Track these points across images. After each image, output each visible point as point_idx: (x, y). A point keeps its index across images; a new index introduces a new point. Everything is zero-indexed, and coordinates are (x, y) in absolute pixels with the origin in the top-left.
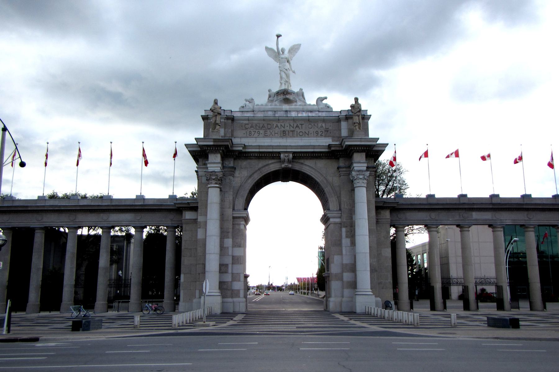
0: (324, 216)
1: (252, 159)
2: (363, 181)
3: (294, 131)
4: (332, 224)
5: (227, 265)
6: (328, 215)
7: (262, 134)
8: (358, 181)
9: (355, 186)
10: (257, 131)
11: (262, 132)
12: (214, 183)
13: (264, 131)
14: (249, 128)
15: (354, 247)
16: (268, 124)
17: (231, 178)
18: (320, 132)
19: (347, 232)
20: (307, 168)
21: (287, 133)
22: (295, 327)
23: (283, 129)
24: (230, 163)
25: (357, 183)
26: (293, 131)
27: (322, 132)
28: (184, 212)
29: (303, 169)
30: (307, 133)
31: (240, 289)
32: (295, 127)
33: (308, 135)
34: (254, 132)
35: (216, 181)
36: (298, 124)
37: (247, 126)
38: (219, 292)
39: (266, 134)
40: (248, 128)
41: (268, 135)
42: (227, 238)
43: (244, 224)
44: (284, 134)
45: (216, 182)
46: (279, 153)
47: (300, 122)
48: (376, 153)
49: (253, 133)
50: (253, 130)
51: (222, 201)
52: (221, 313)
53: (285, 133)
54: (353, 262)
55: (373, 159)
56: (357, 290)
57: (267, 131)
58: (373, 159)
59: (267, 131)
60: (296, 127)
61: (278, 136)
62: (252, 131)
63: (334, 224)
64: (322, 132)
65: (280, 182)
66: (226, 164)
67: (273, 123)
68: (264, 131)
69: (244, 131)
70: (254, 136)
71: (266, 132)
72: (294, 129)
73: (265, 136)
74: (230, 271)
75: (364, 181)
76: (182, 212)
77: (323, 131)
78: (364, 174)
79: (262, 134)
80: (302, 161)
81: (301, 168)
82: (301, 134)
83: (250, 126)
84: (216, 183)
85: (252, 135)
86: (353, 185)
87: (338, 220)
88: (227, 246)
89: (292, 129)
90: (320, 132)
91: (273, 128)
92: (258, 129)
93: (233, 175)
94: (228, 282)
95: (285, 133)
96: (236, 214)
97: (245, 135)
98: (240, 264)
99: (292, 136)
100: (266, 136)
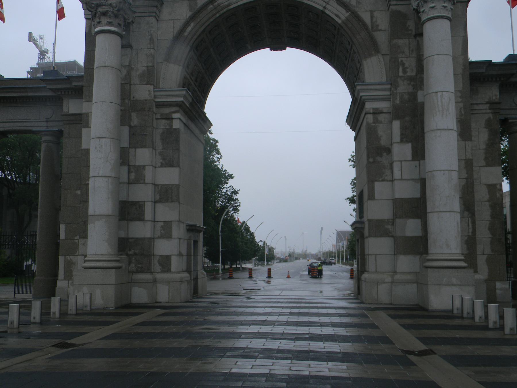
0: (353, 105)
2: (443, 5)
4: (370, 113)
5: (139, 206)
6: (362, 94)
8: (432, 5)
9: (424, 17)
12: (106, 22)
15: (422, 162)
17: (152, 20)
19: (403, 128)
25: (427, 12)
28: (65, 102)
31: (171, 255)
35: (110, 18)
42: (142, 148)
43: (180, 119)
45: (109, 20)
52: (116, 308)
54: (418, 195)
56: (430, 257)
63: (374, 113)
65: (267, 51)
74: (148, 215)
75: (445, 5)
76: (63, 100)
84: (110, 24)
86: (420, 18)
87: (383, 105)
88: (142, 164)
93: (154, 14)
94: (144, 239)
96: (161, 96)
98: (172, 202)
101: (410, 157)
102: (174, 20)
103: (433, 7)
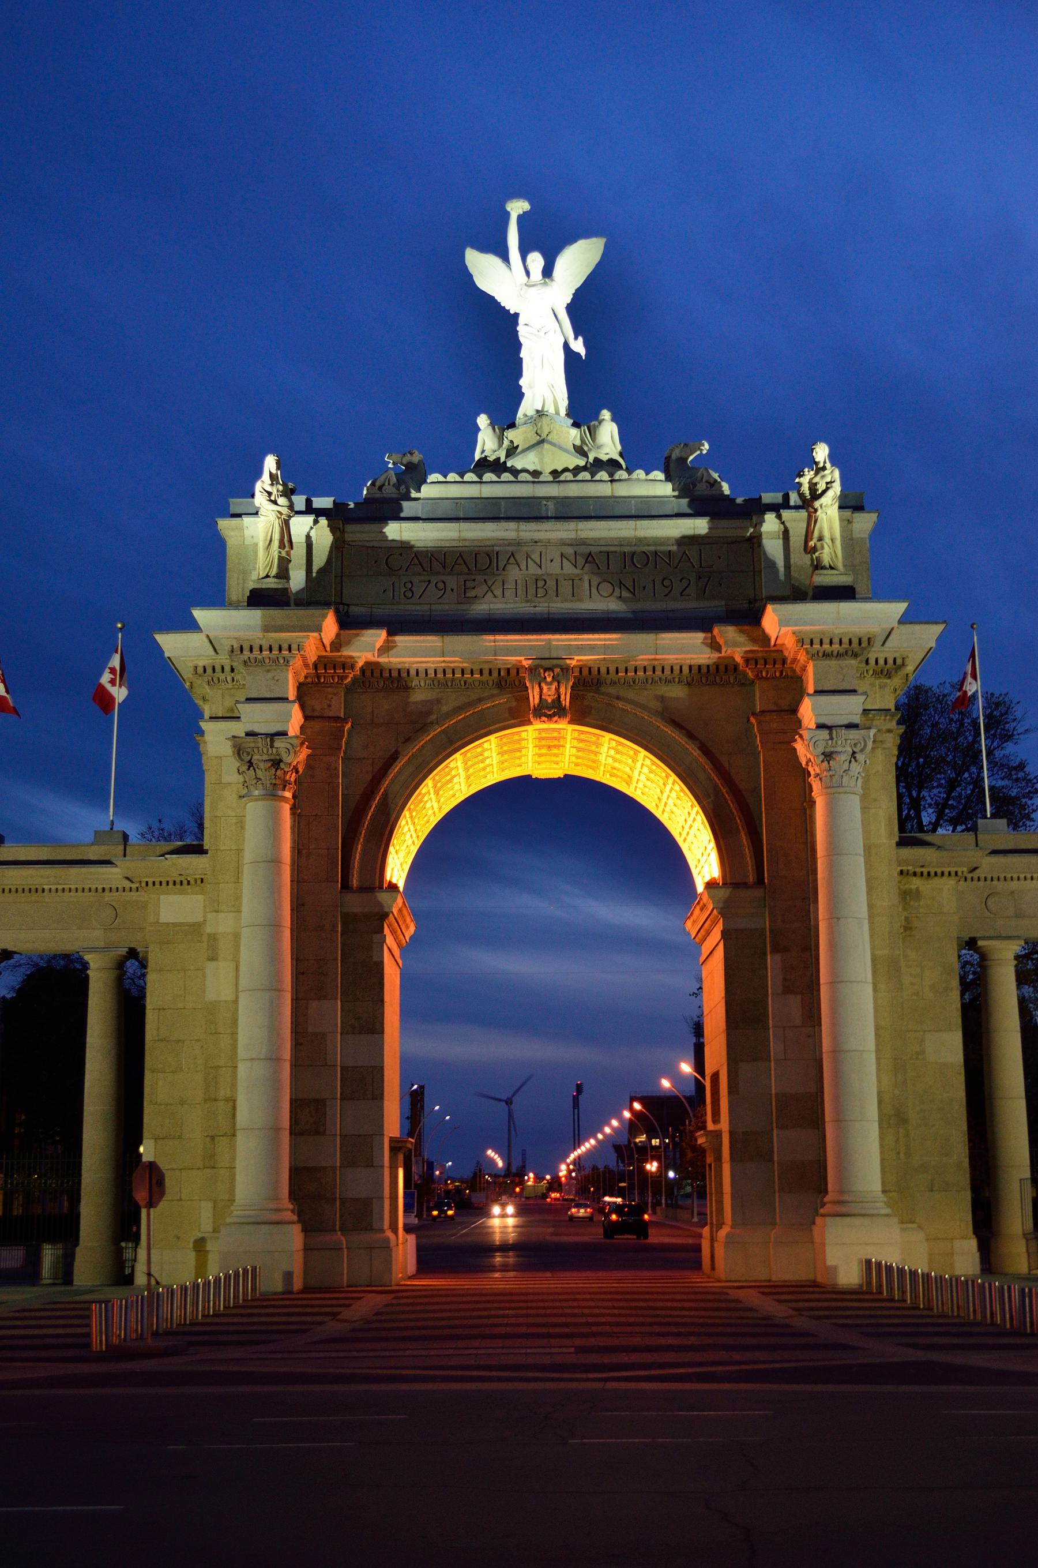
7: (452, 590)
11: (452, 582)
13: (462, 578)
21: (551, 583)
22: (572, 1350)
23: (534, 570)
24: (329, 706)
27: (685, 583)
31: (372, 1198)
38: (293, 1211)
40: (401, 568)
51: (299, 851)
62: (416, 580)
64: (685, 583)
66: (314, 710)
68: (462, 578)
79: (452, 590)
91: (497, 570)
92: (438, 573)
101: (798, 1021)
102: (373, 759)
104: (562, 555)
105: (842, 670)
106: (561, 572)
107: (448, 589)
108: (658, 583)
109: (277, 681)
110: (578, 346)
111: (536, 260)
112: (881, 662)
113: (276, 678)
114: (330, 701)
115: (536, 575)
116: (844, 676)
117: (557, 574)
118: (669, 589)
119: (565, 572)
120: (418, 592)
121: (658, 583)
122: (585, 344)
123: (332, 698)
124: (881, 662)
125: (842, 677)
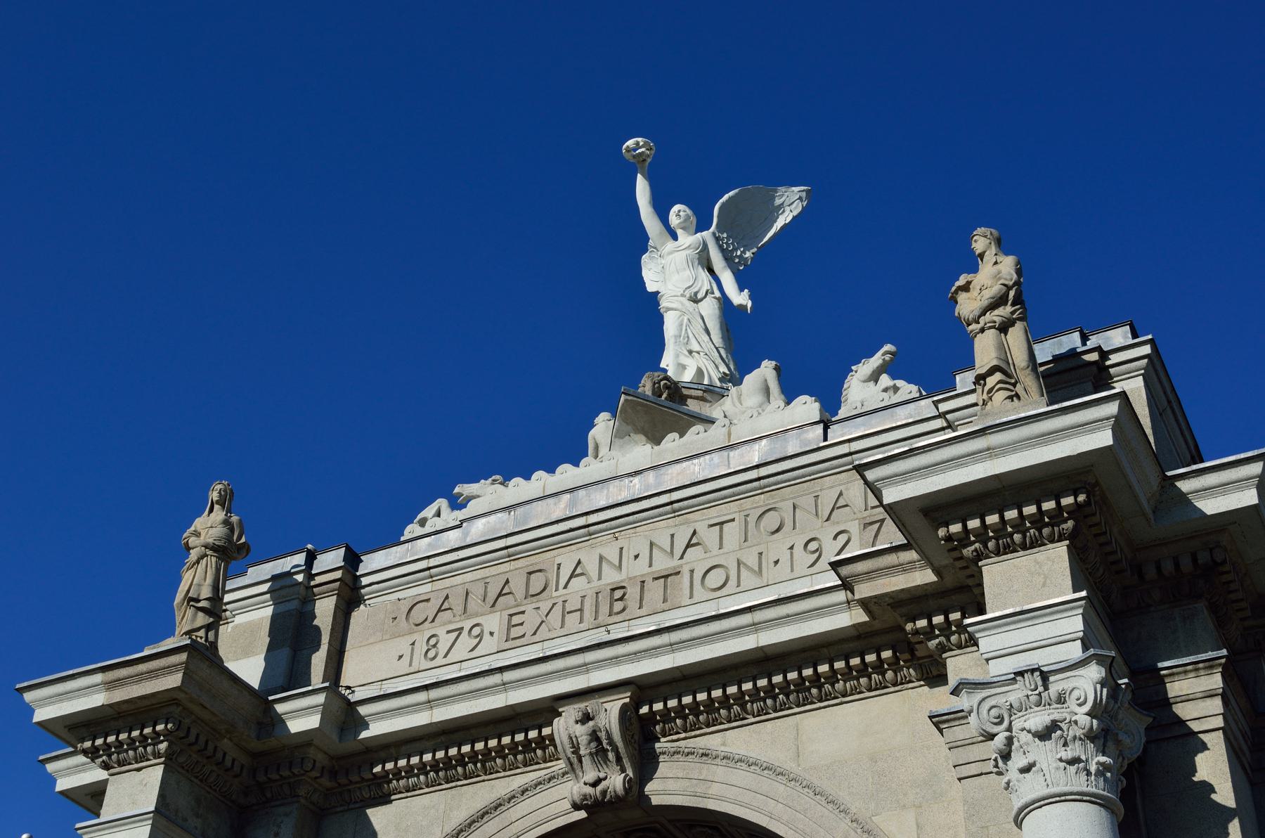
1: (415, 788)
3: (678, 573)
7: (492, 634)
8: (1023, 762)
10: (467, 625)
11: (494, 622)
14: (430, 619)
16: (530, 573)
18: (835, 538)
20: (741, 776)
21: (633, 592)
23: (611, 577)
26: (666, 577)
27: (842, 539)
29: (715, 789)
30: (752, 561)
32: (678, 552)
33: (760, 572)
34: (455, 634)
36: (701, 528)
37: (418, 614)
39: (515, 632)
40: (426, 620)
41: (524, 636)
44: (618, 606)
46: (547, 710)
47: (713, 512)
48: (1203, 557)
49: (445, 641)
50: (450, 622)
53: (621, 599)
55: (1201, 605)
57: (523, 612)
58: (1201, 605)
59: (523, 612)
60: (689, 546)
61: (583, 626)
62: (441, 632)
64: (842, 539)
67: (558, 560)
69: (403, 645)
70: (450, 659)
71: (516, 620)
72: (673, 563)
73: (511, 644)
77: (854, 528)
78: (1061, 699)
79: (492, 634)
80: (712, 741)
81: (700, 789)
82: (715, 579)
83: (431, 609)
85: (442, 653)
89: (663, 563)
90: (835, 538)
95: (621, 599)
97: (406, 659)
99: (661, 606)
100: (518, 643)
103: (1026, 770)
104: (652, 544)
105: (1040, 568)
106: (648, 570)
107: (486, 636)
108: (799, 549)
109: (146, 785)
110: (741, 298)
111: (678, 214)
112: (1168, 567)
113: (144, 783)
114: (279, 827)
115: (608, 584)
116: (1046, 578)
117: (642, 576)
118: (817, 554)
119: (654, 568)
120: (443, 647)
121: (799, 549)
122: (751, 297)
123: (282, 822)
124: (1168, 567)
125: (1041, 579)
